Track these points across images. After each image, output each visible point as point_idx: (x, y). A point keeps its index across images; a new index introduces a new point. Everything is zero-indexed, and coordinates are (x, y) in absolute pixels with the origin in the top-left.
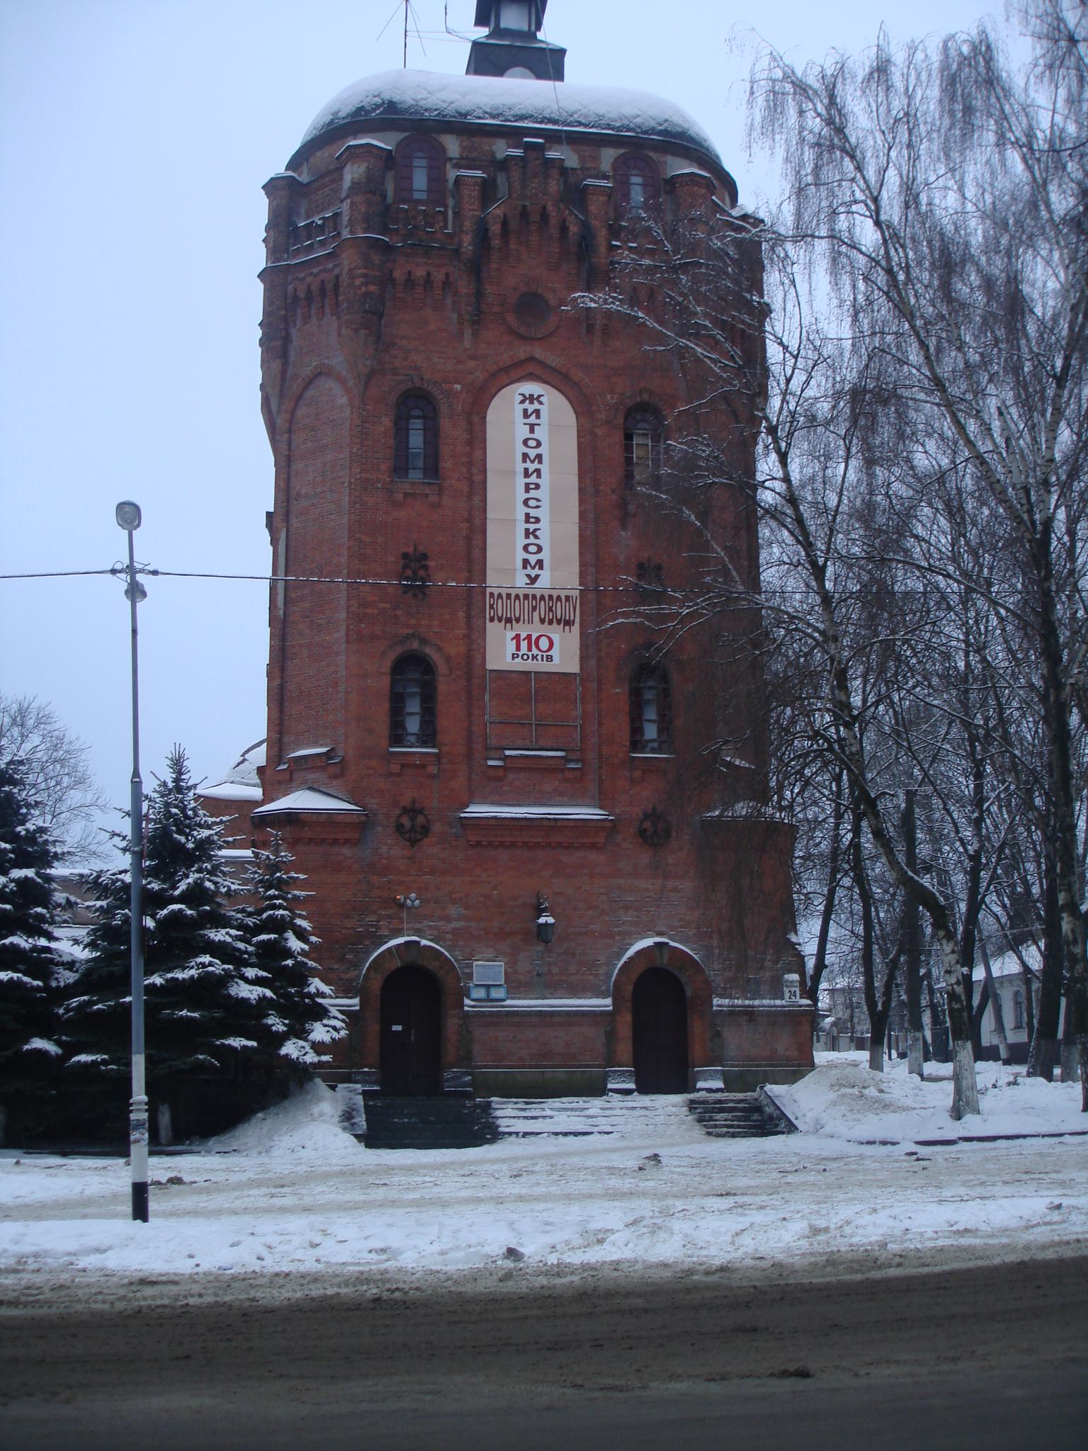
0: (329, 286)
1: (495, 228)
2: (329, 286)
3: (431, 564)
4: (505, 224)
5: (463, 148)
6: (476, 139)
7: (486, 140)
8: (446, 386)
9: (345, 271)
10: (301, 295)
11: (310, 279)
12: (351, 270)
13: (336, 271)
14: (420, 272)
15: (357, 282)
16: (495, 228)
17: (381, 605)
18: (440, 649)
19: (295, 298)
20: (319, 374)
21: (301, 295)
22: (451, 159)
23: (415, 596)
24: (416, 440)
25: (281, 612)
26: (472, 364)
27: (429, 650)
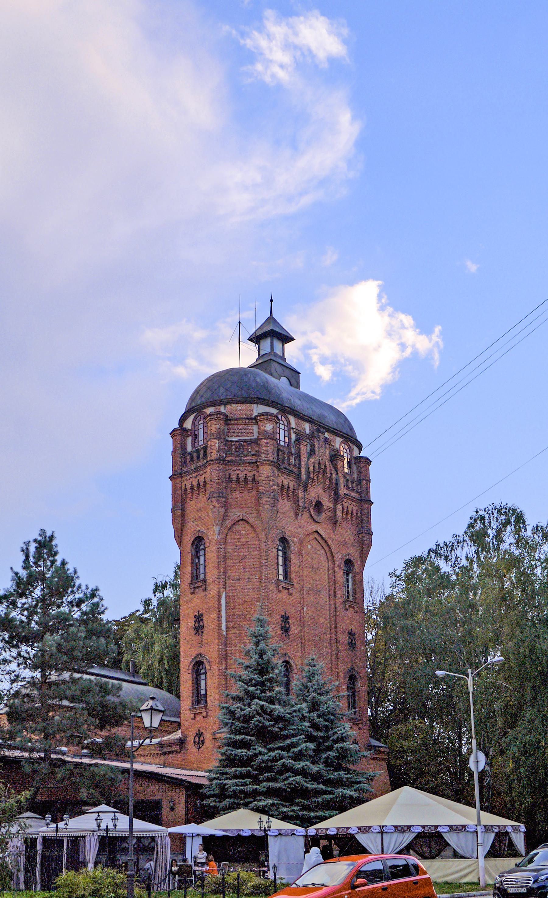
0: (250, 479)
1: (311, 468)
2: (250, 479)
3: (290, 621)
4: (314, 467)
5: (296, 424)
6: (300, 421)
7: (303, 422)
8: (292, 538)
9: (263, 476)
10: (234, 477)
11: (238, 472)
12: (268, 477)
13: (253, 472)
14: (286, 482)
15: (271, 483)
16: (311, 468)
17: (276, 638)
18: (294, 662)
19: (229, 478)
20: (243, 520)
21: (234, 477)
22: (293, 428)
23: (286, 636)
24: (281, 559)
25: (225, 633)
26: (300, 530)
27: (291, 662)
